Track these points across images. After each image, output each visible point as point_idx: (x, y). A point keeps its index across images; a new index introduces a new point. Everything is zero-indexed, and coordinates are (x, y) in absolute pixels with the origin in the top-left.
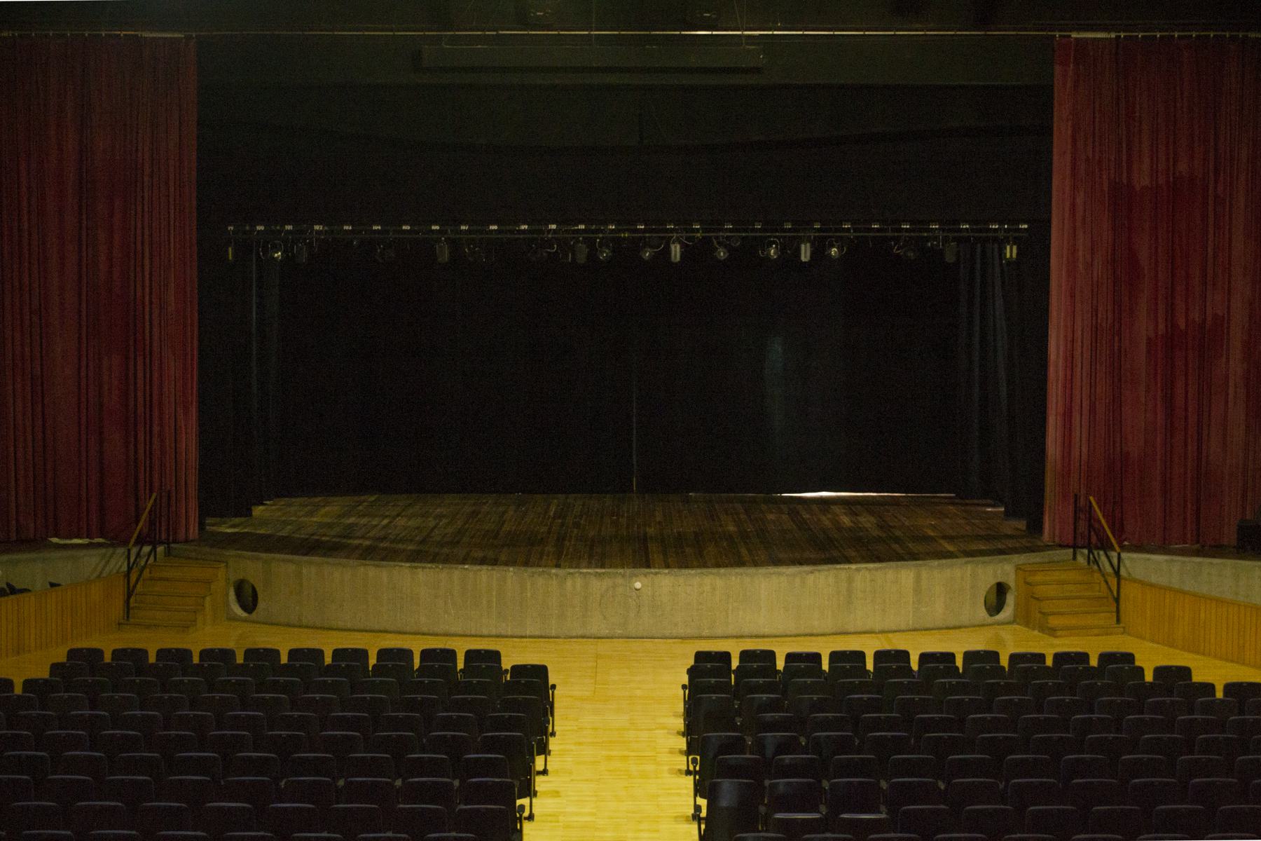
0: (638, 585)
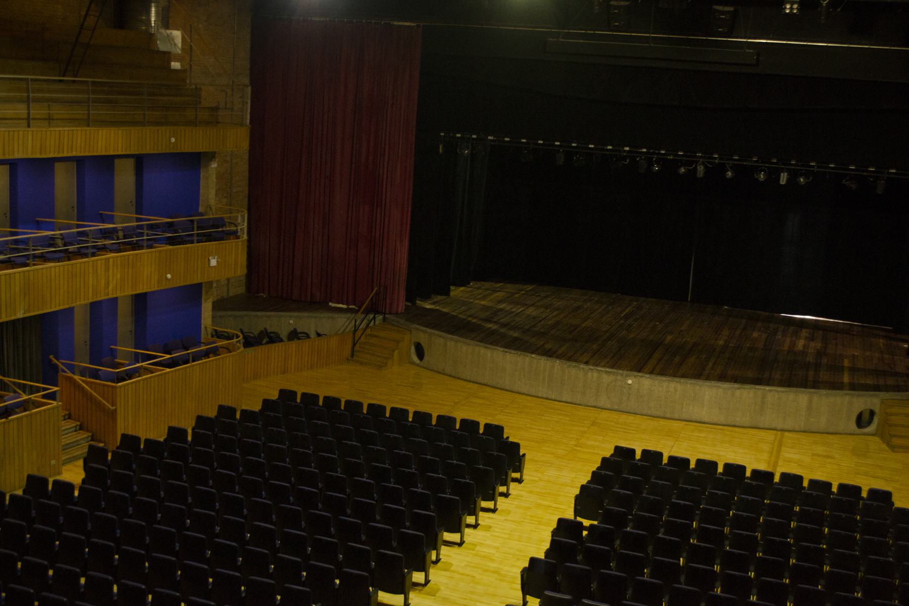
0: (630, 382)
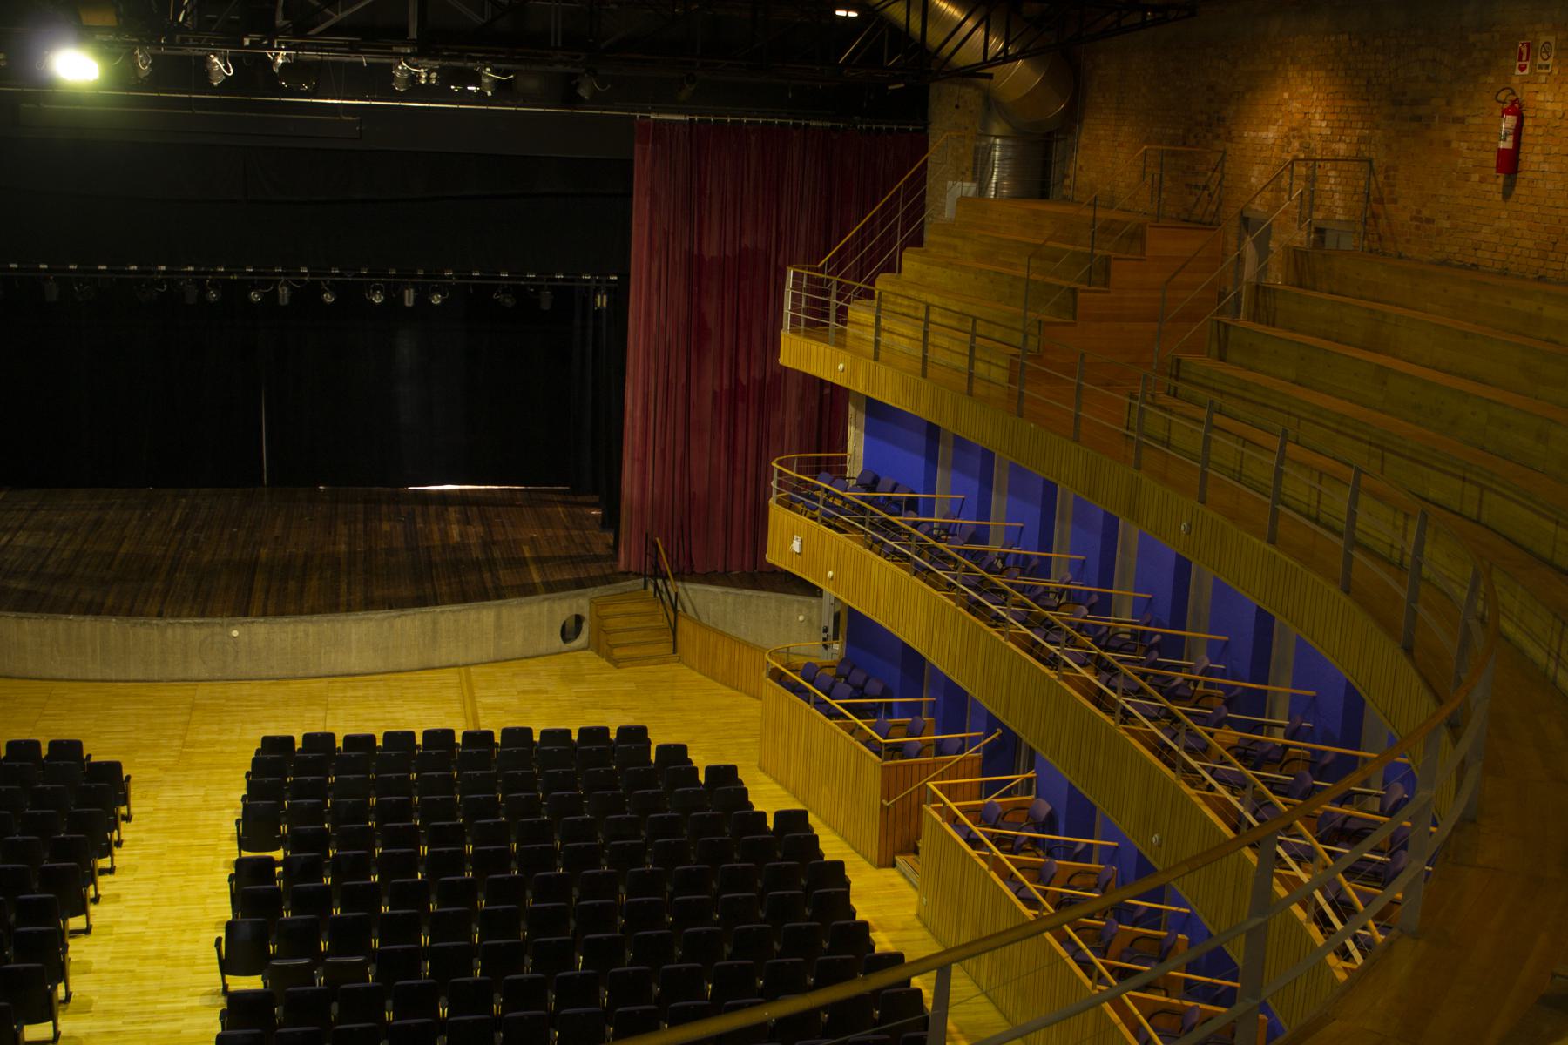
0: (235, 633)
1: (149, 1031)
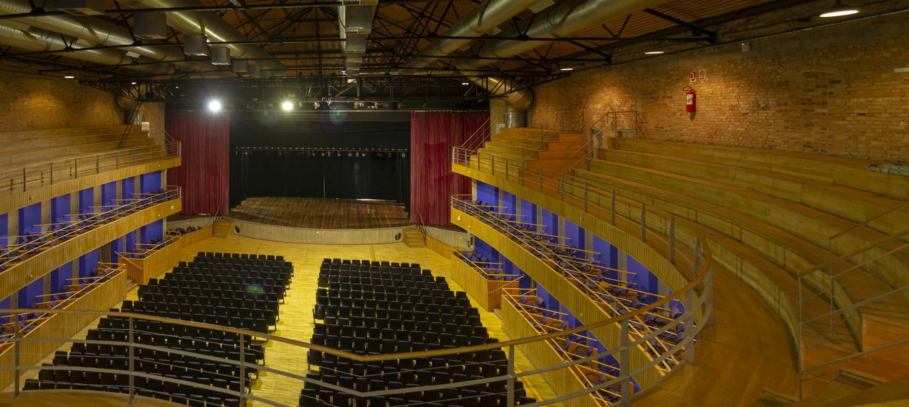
1: (296, 331)
